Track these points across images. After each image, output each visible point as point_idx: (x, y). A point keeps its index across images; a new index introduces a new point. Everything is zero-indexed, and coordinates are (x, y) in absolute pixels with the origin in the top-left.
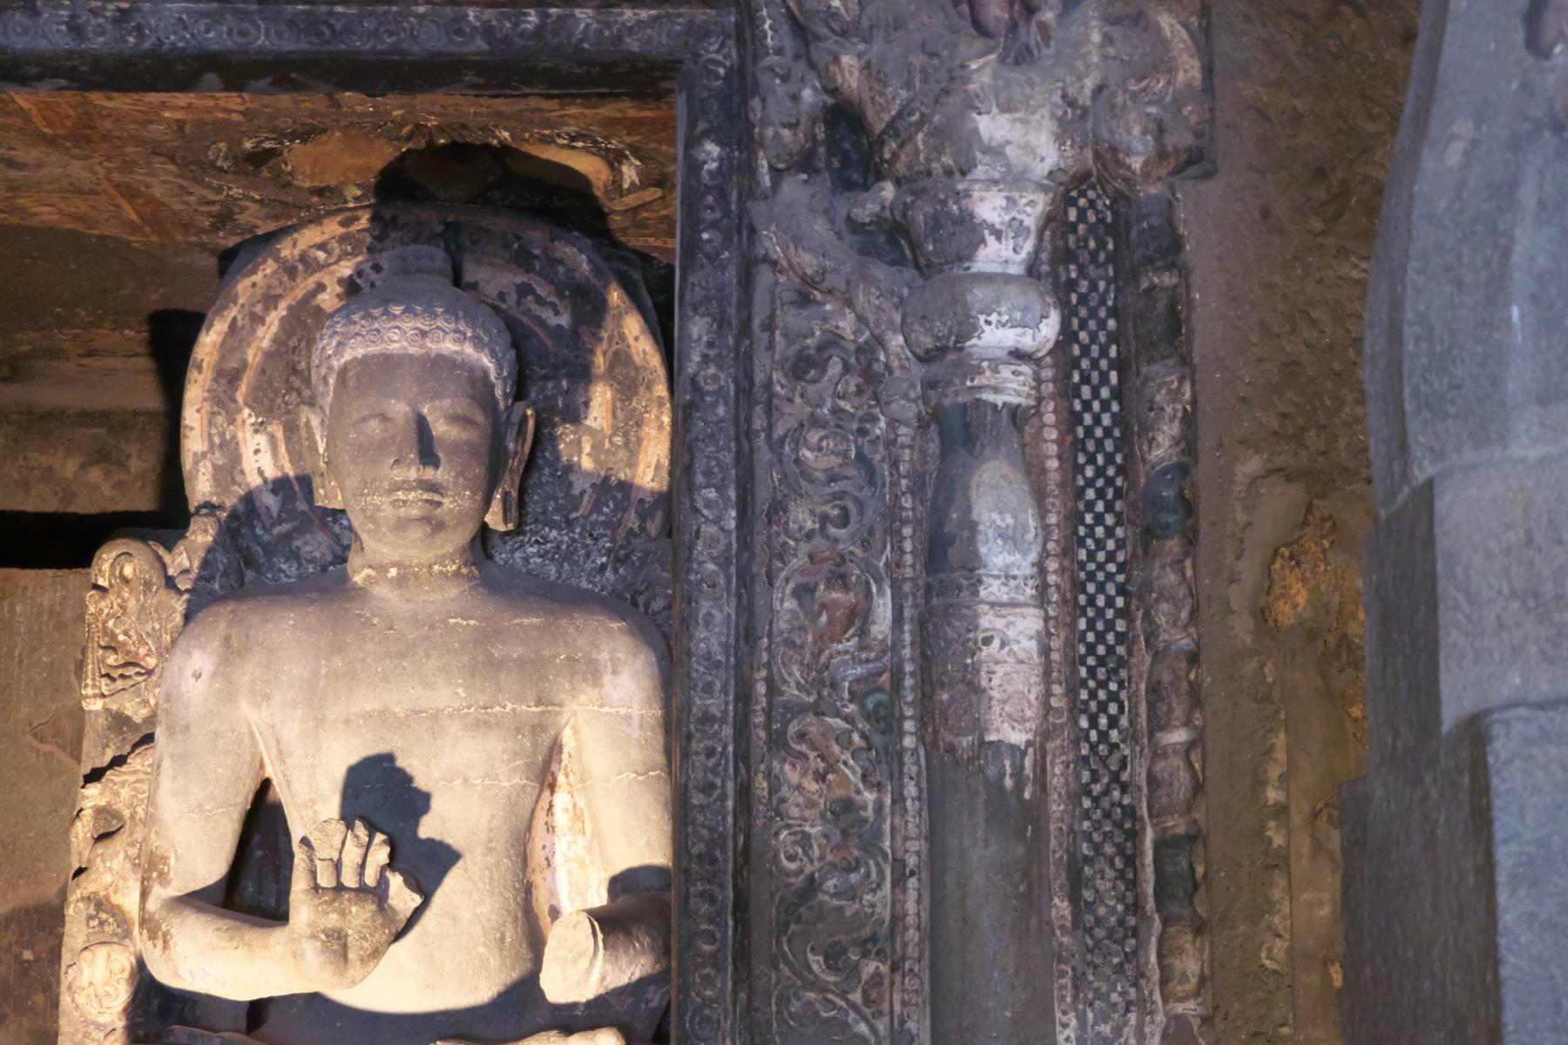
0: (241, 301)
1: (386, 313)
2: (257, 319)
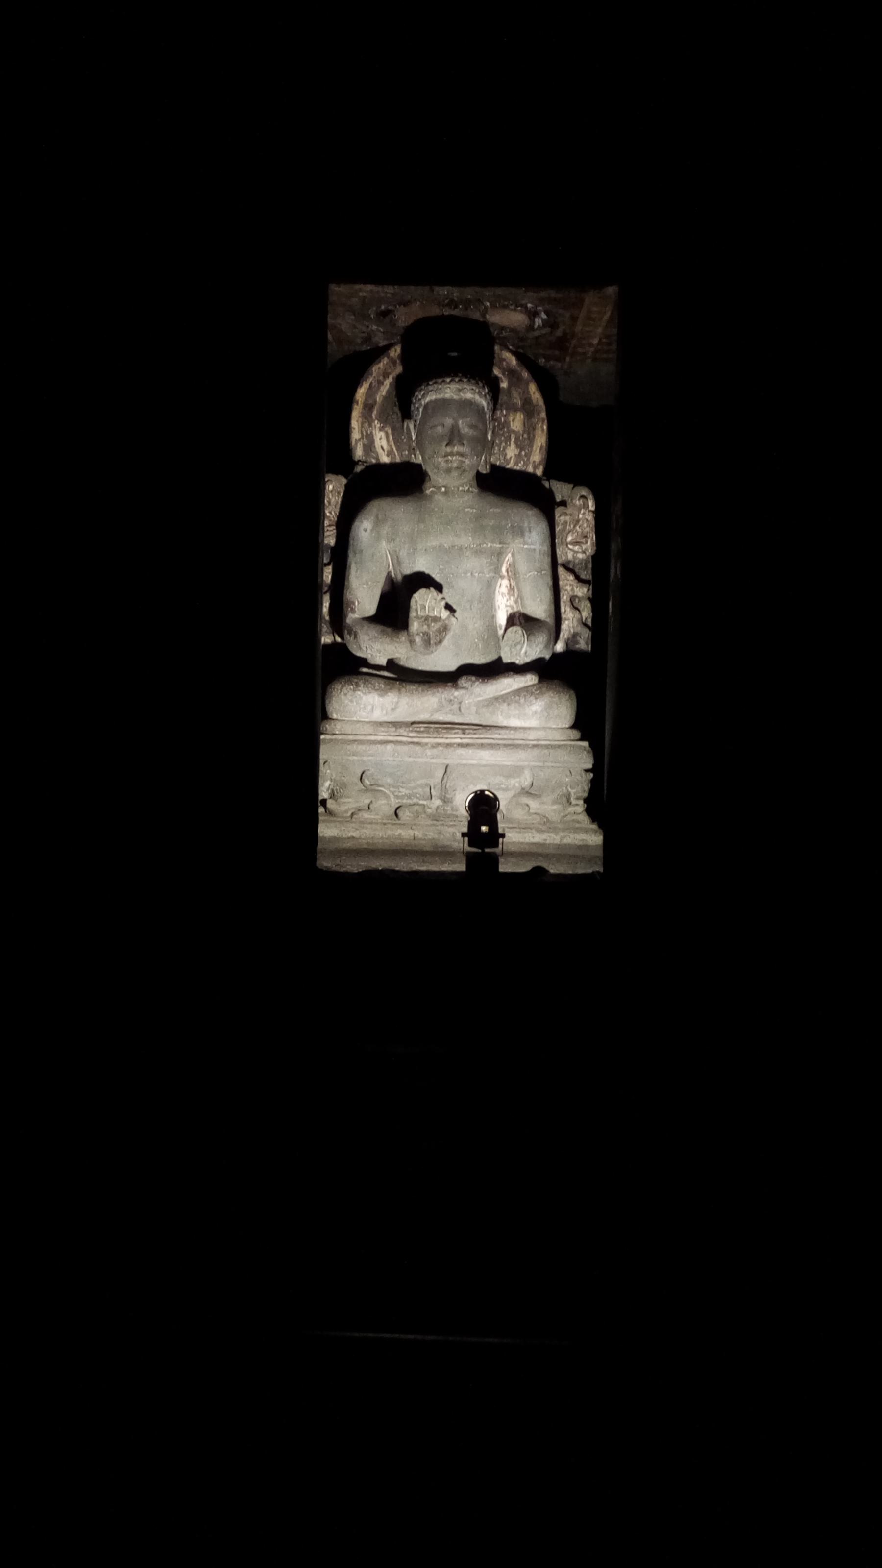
0: (374, 374)
1: (444, 381)
2: (380, 383)
